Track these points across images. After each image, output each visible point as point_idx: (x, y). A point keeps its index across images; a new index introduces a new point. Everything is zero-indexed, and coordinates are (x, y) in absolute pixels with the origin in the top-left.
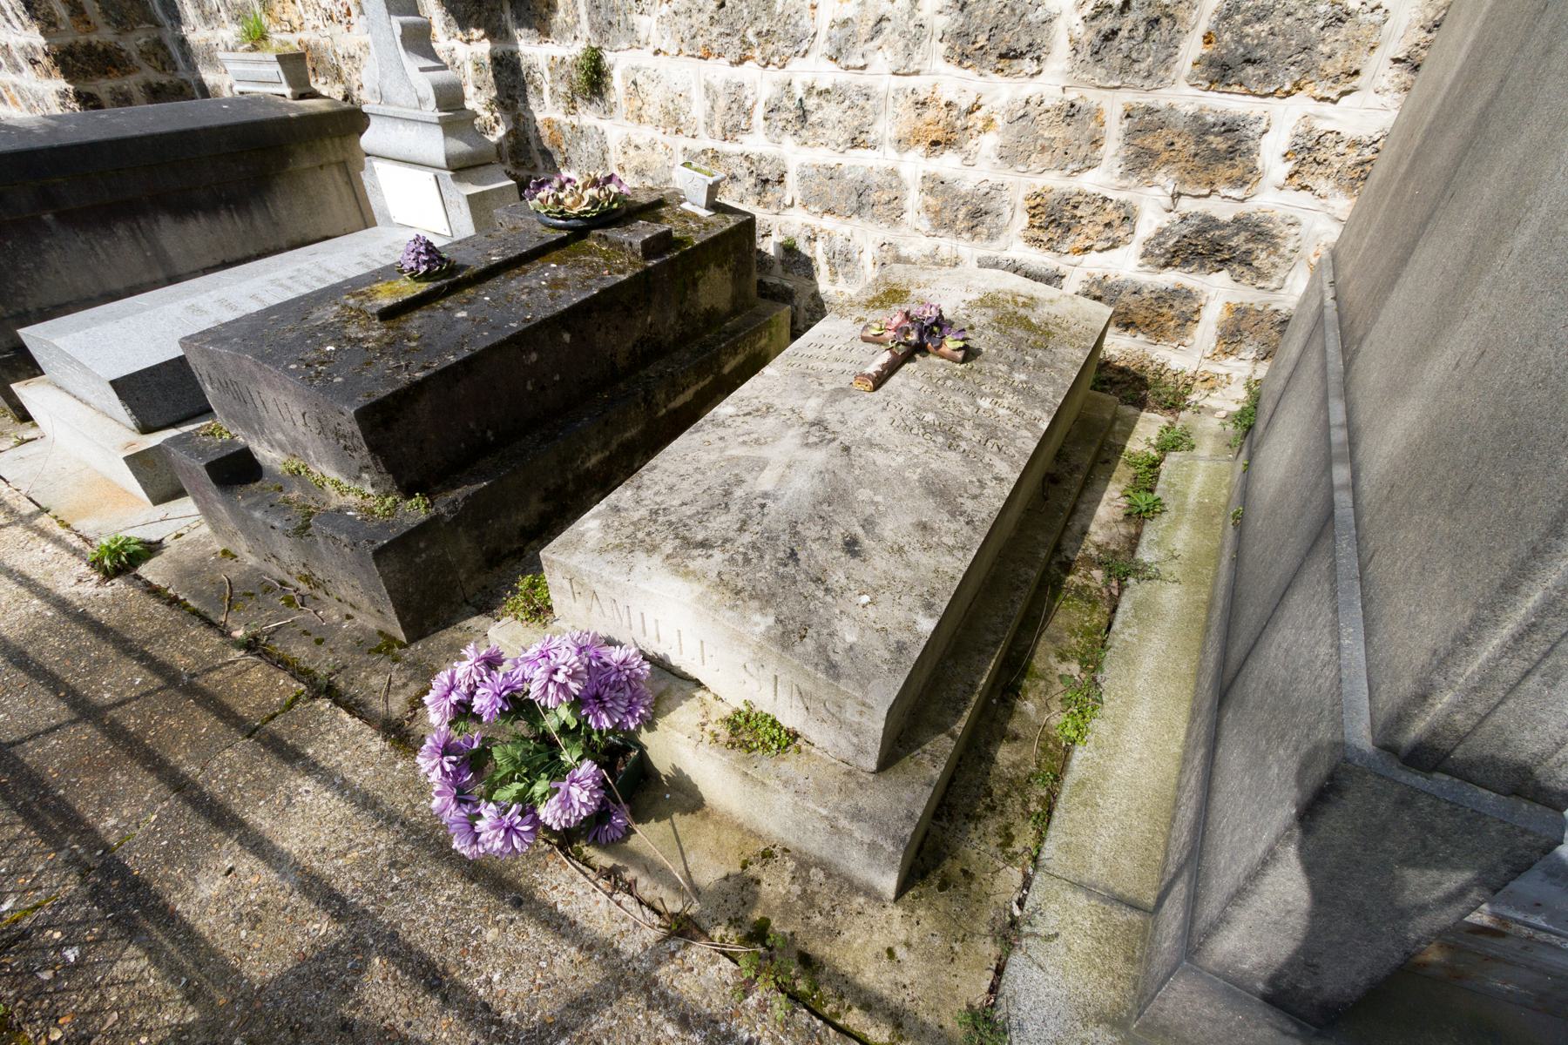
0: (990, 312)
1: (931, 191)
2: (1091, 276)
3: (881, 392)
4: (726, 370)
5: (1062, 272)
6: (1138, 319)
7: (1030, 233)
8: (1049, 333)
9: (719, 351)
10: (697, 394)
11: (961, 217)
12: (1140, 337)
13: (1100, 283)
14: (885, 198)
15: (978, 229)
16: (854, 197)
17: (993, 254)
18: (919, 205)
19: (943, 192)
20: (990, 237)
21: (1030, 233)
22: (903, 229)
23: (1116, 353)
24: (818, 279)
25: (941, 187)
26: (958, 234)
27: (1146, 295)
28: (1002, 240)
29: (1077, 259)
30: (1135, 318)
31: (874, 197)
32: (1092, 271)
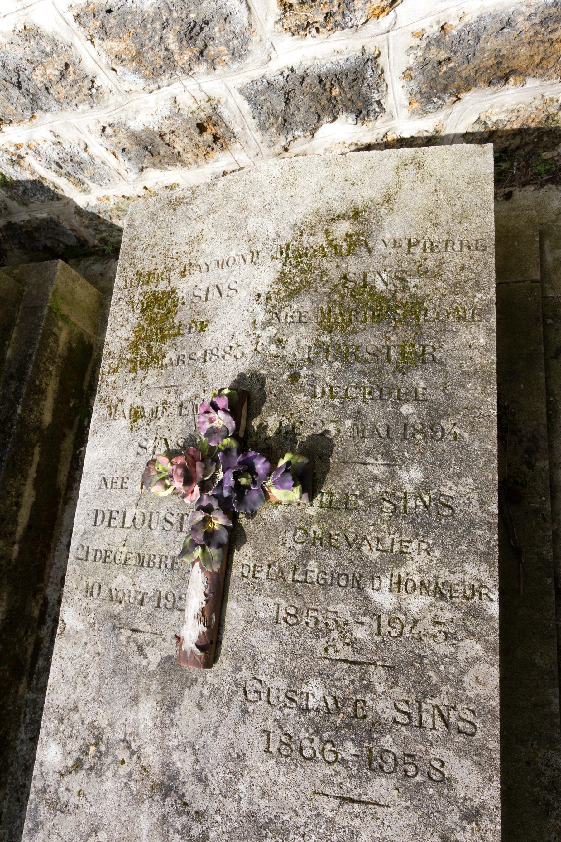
0: (305, 304)
1: (105, 32)
2: (419, 35)
3: (224, 663)
4: (47, 418)
5: (371, 51)
6: (521, 63)
7: (291, 21)
8: (416, 306)
9: (22, 420)
10: (37, 484)
11: (173, 47)
12: (531, 83)
13: (439, 42)
14: (53, 72)
15: (212, 50)
16: (15, 92)
17: (257, 74)
18: (104, 60)
19: (123, 24)
20: (237, 55)
21: (291, 21)
22: (112, 100)
23: (502, 117)
24: (67, 195)
25: (112, 20)
26: (188, 71)
27: (521, 24)
28: (257, 52)
29: (386, 21)
30: (514, 64)
31: (38, 78)
32: (417, 28)
